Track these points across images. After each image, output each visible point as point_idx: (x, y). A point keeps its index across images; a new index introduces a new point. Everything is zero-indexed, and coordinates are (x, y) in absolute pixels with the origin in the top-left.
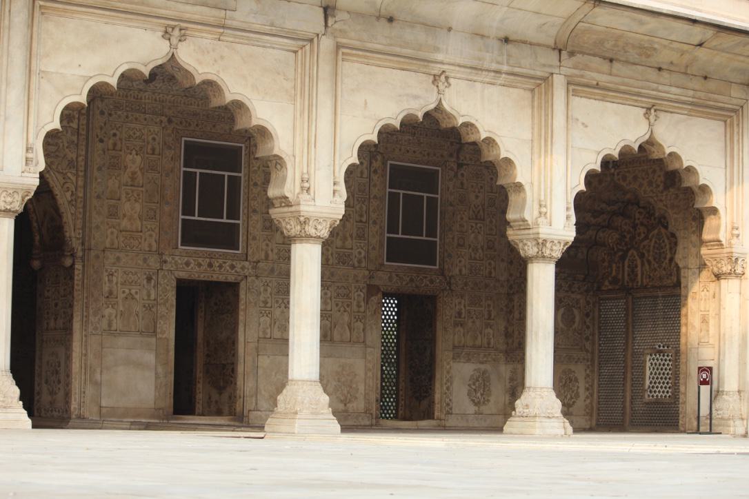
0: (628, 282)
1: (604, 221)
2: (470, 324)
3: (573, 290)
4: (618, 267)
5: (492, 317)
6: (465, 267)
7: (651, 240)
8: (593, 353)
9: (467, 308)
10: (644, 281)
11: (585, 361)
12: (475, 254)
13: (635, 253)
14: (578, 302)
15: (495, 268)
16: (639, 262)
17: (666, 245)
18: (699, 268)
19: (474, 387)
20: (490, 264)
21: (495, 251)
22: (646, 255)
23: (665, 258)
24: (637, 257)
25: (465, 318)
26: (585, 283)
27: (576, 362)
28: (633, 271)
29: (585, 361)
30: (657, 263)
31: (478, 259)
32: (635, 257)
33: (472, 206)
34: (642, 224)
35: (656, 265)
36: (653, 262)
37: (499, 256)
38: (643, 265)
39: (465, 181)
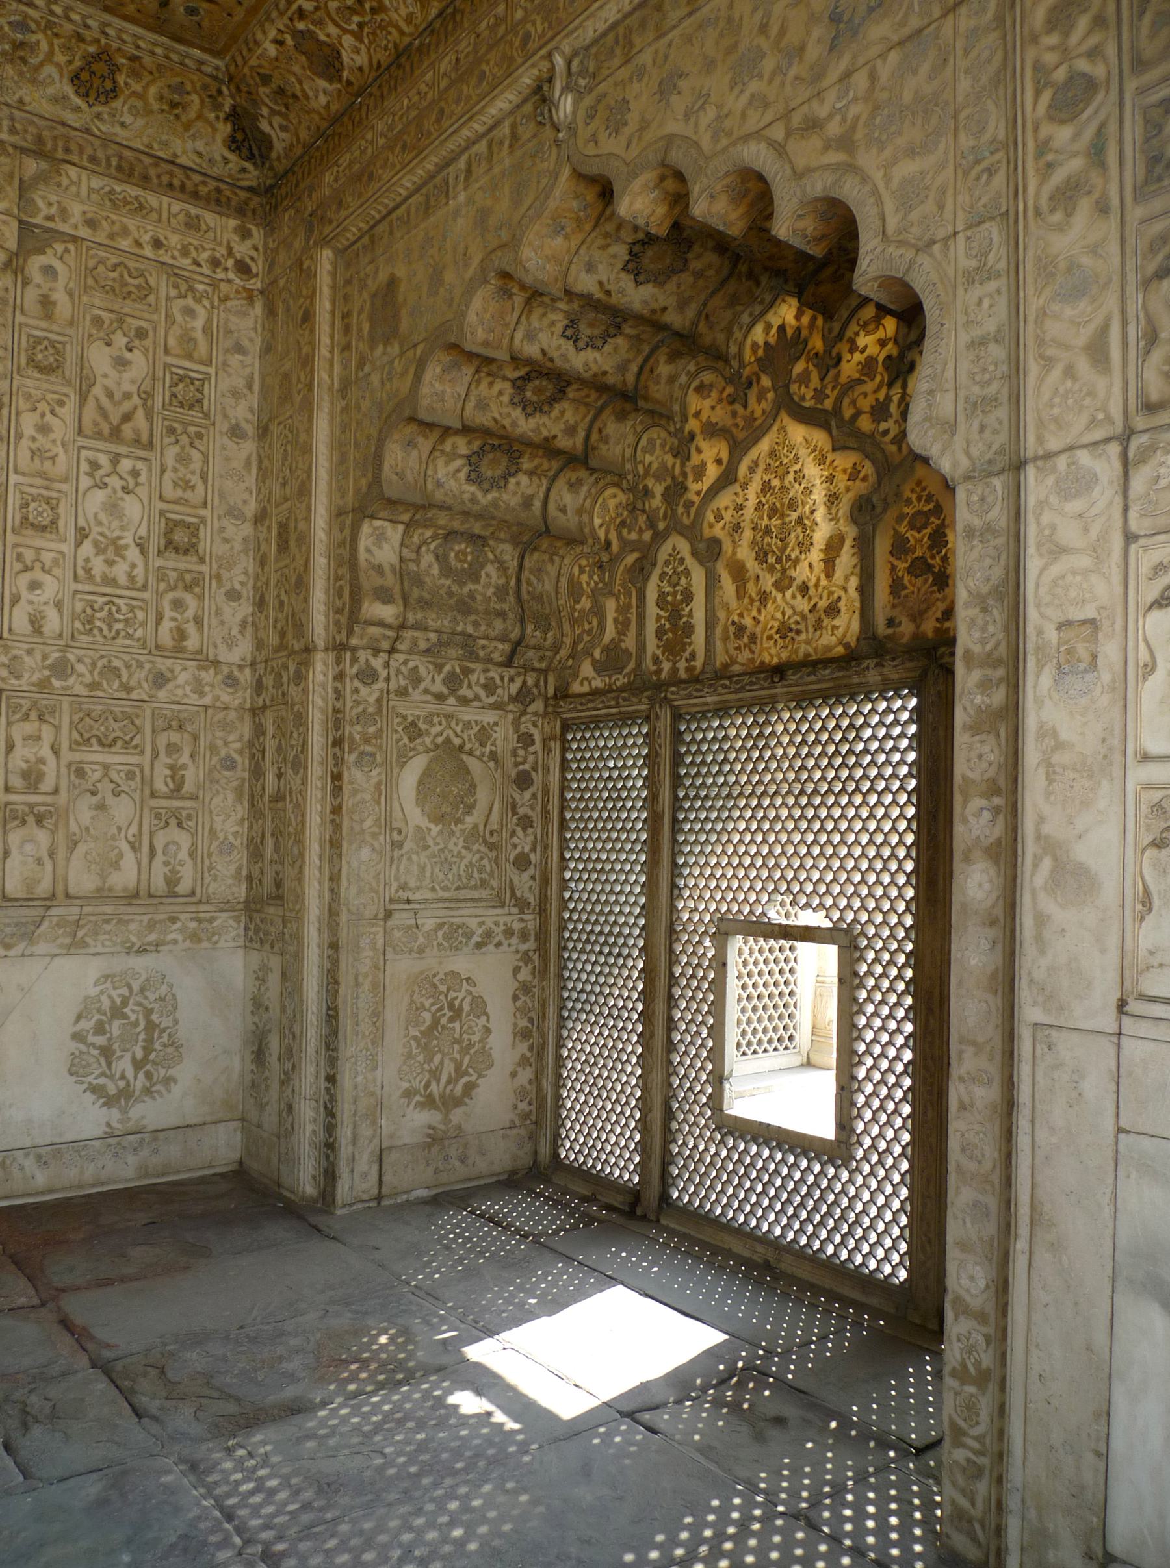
0: (656, 661)
1: (571, 431)
2: (83, 812)
3: (464, 692)
4: (623, 610)
5: (188, 787)
6: (58, 605)
7: (744, 487)
8: (542, 911)
9: (67, 756)
10: (719, 645)
11: (514, 940)
12: (110, 563)
13: (684, 547)
14: (484, 735)
15: (198, 621)
16: (698, 579)
17: (808, 491)
18: (1126, 436)
19: (100, 1040)
20: (178, 604)
21: (202, 560)
22: (727, 546)
23: (805, 546)
24: (690, 561)
25: (56, 791)
26: (512, 671)
27: (479, 945)
28: (676, 616)
29: (514, 940)
30: (771, 569)
31: (123, 580)
32: (682, 560)
33: (97, 390)
34: (712, 431)
35: (768, 582)
36: (752, 565)
37: (218, 577)
38: (712, 583)
39: (60, 296)
